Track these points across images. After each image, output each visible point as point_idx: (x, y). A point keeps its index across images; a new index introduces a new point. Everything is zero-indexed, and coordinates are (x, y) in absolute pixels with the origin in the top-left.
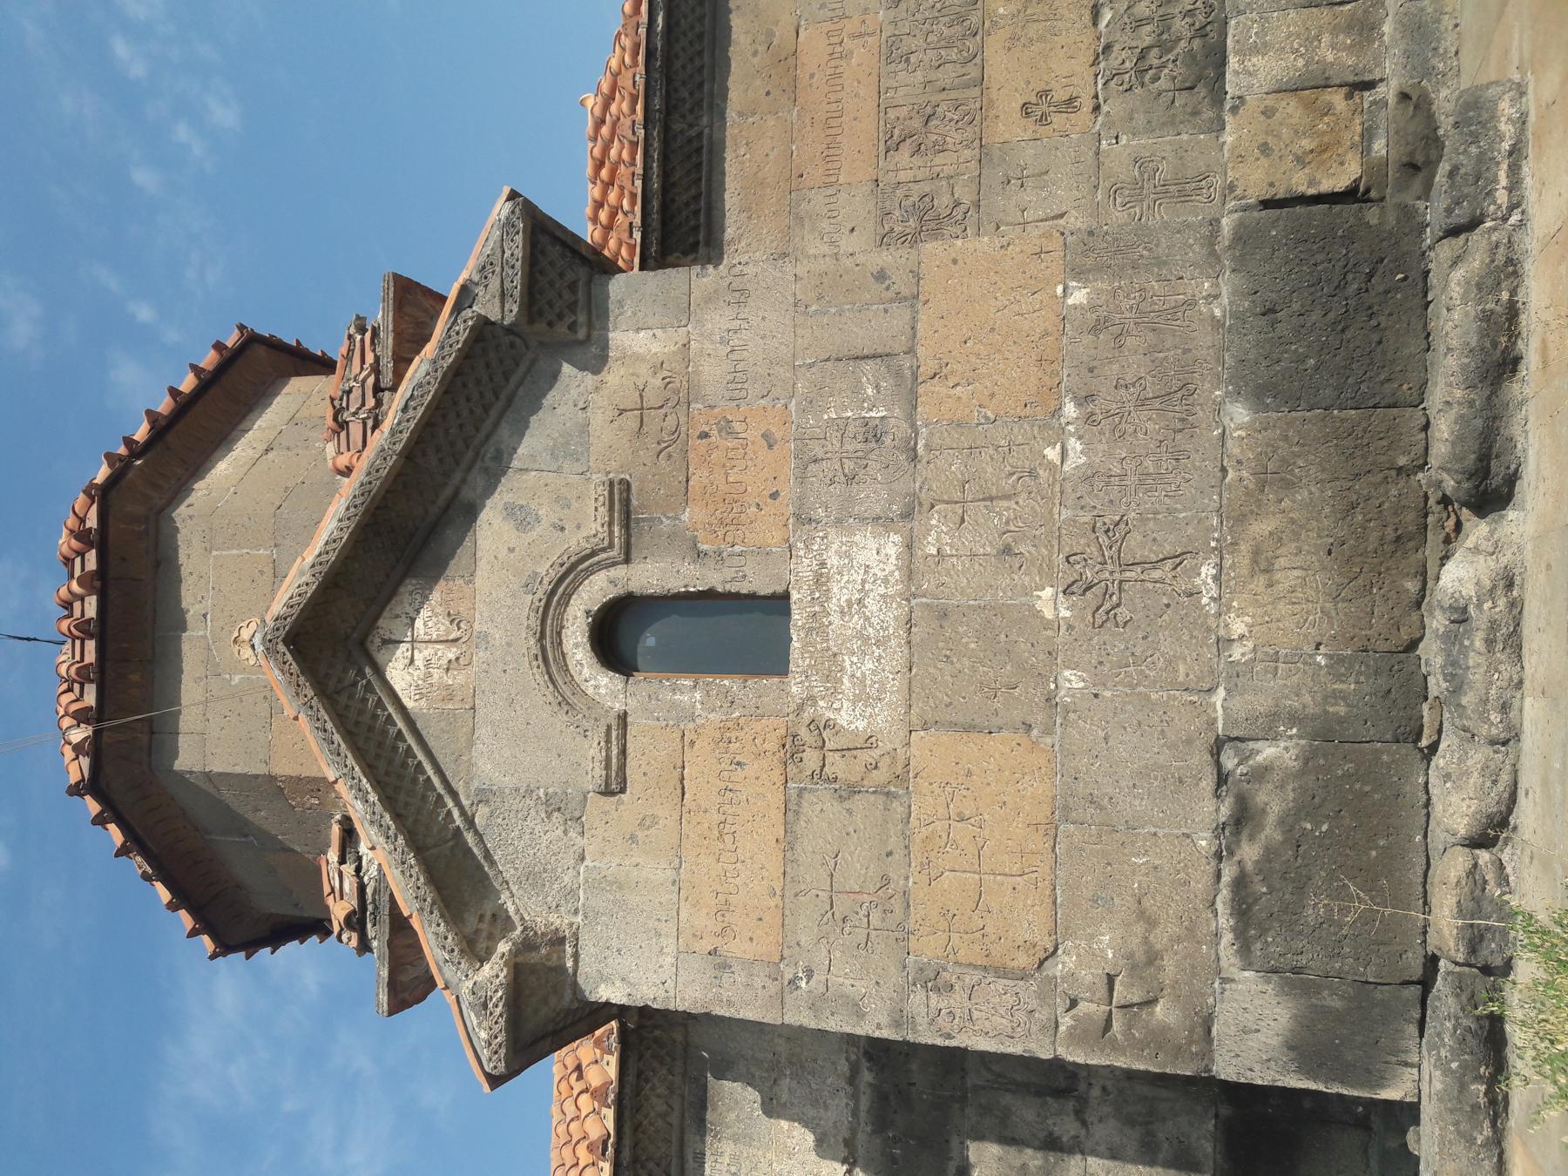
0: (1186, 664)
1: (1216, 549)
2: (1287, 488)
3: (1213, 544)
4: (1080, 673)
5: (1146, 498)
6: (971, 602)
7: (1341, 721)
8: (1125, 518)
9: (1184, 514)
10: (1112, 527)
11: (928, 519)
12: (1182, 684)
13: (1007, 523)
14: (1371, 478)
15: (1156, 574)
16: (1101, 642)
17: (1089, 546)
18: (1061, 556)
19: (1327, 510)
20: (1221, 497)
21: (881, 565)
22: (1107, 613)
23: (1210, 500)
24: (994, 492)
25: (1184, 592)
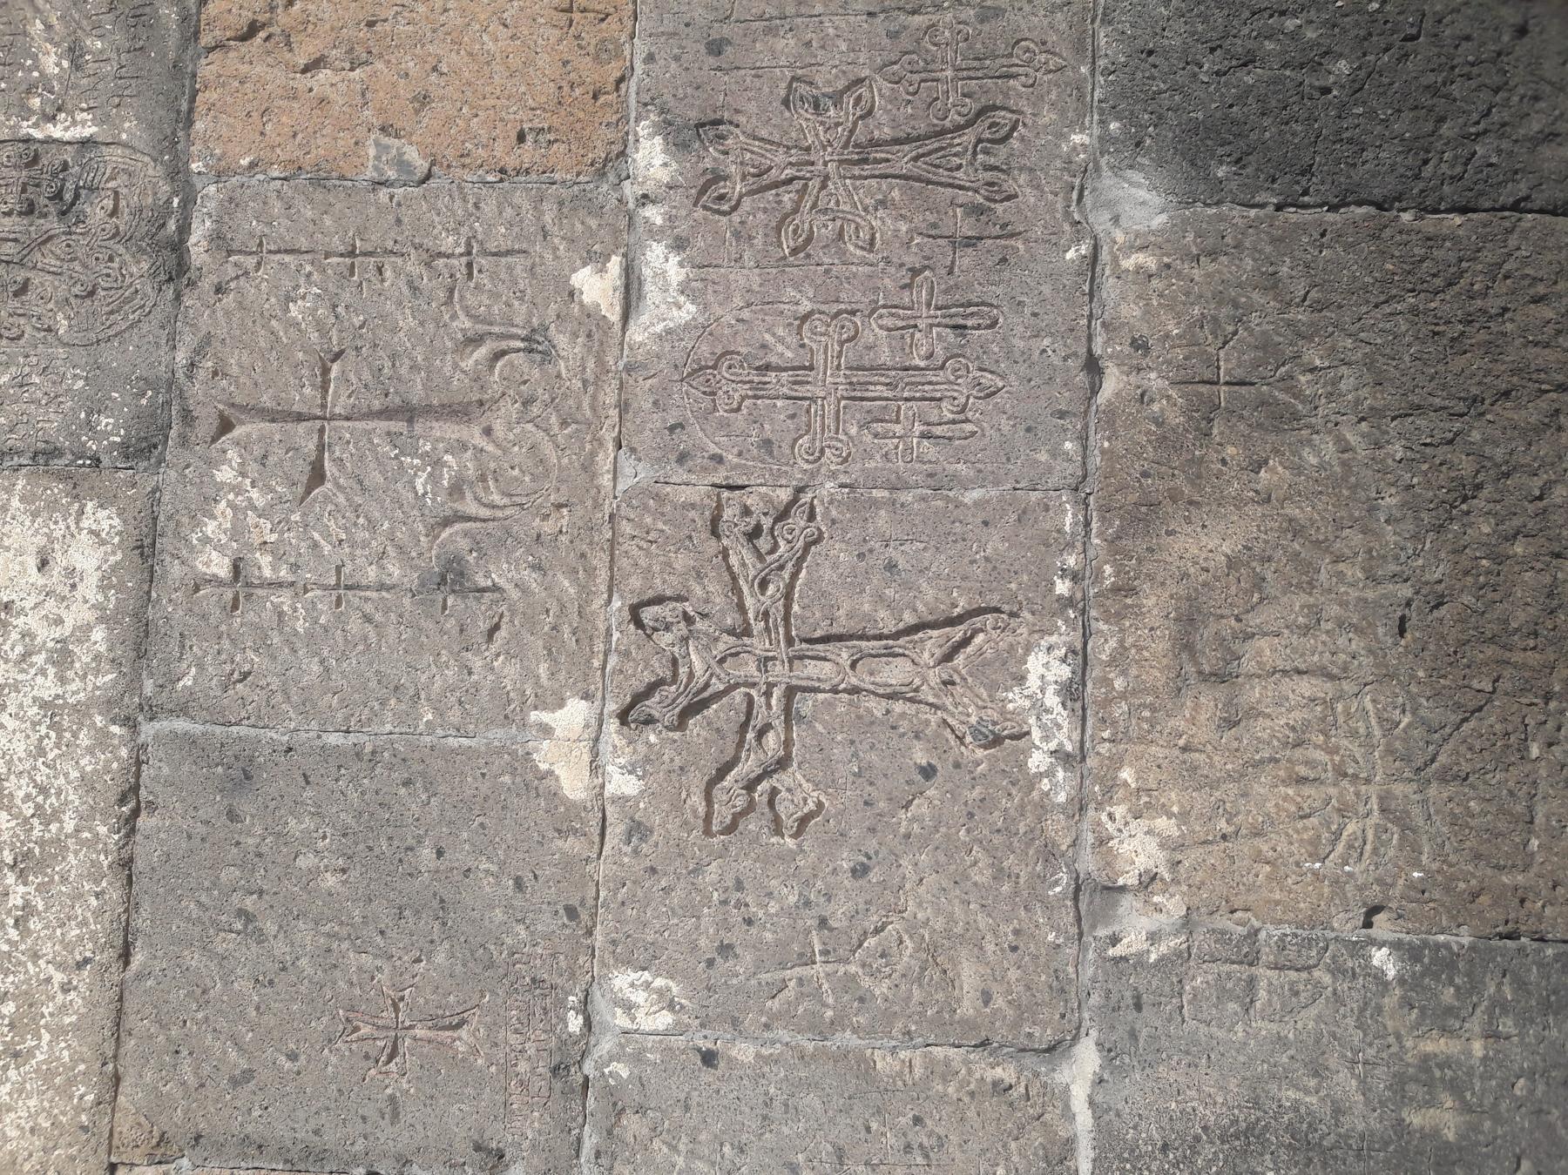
0: (981, 958)
1: (1069, 602)
2: (1278, 430)
3: (1062, 587)
4: (659, 982)
5: (868, 438)
6: (333, 739)
7: (1447, 1156)
8: (806, 498)
9: (975, 494)
10: (767, 523)
11: (212, 463)
12: (969, 1025)
13: (456, 490)
14: (1507, 412)
15: (895, 673)
16: (730, 883)
17: (699, 576)
18: (617, 603)
19: (1390, 501)
20: (1085, 448)
21: (51, 603)
22: (750, 787)
23: (1054, 456)
24: (417, 393)
25: (976, 732)
